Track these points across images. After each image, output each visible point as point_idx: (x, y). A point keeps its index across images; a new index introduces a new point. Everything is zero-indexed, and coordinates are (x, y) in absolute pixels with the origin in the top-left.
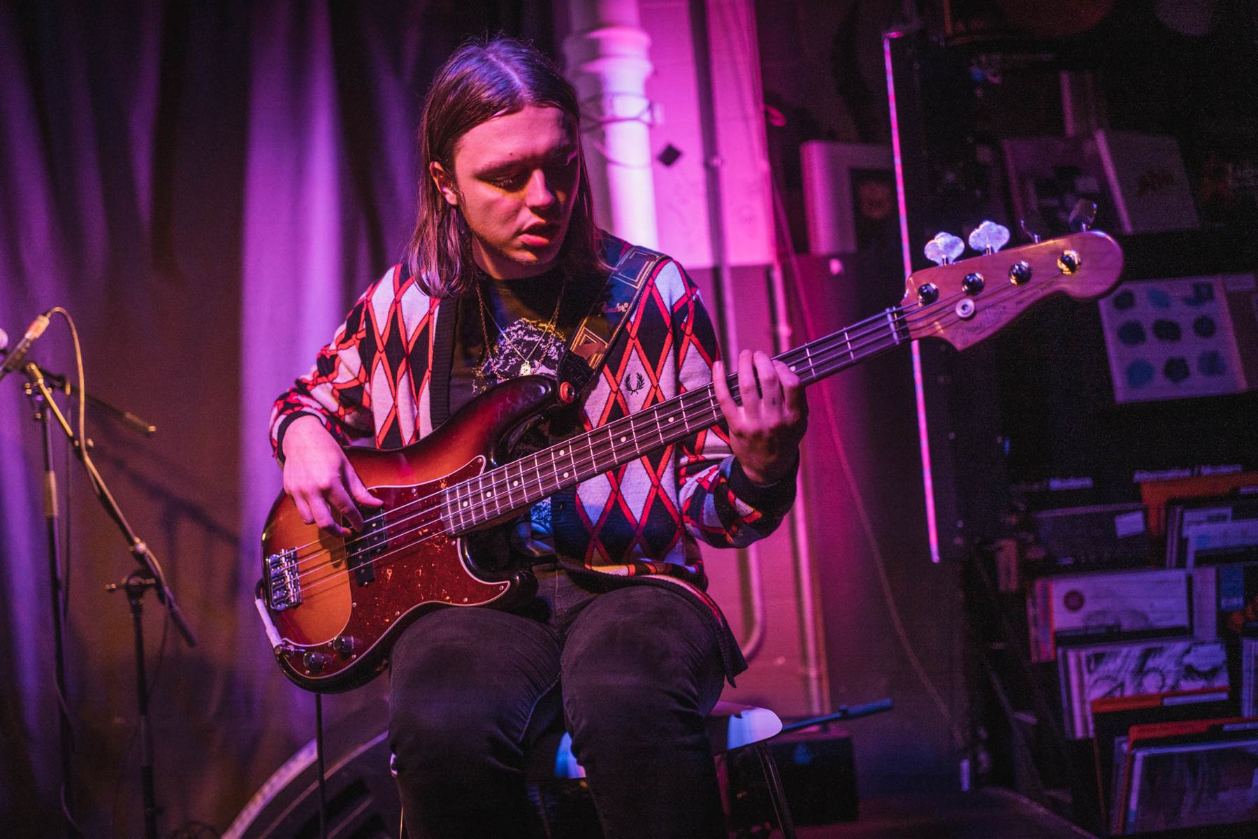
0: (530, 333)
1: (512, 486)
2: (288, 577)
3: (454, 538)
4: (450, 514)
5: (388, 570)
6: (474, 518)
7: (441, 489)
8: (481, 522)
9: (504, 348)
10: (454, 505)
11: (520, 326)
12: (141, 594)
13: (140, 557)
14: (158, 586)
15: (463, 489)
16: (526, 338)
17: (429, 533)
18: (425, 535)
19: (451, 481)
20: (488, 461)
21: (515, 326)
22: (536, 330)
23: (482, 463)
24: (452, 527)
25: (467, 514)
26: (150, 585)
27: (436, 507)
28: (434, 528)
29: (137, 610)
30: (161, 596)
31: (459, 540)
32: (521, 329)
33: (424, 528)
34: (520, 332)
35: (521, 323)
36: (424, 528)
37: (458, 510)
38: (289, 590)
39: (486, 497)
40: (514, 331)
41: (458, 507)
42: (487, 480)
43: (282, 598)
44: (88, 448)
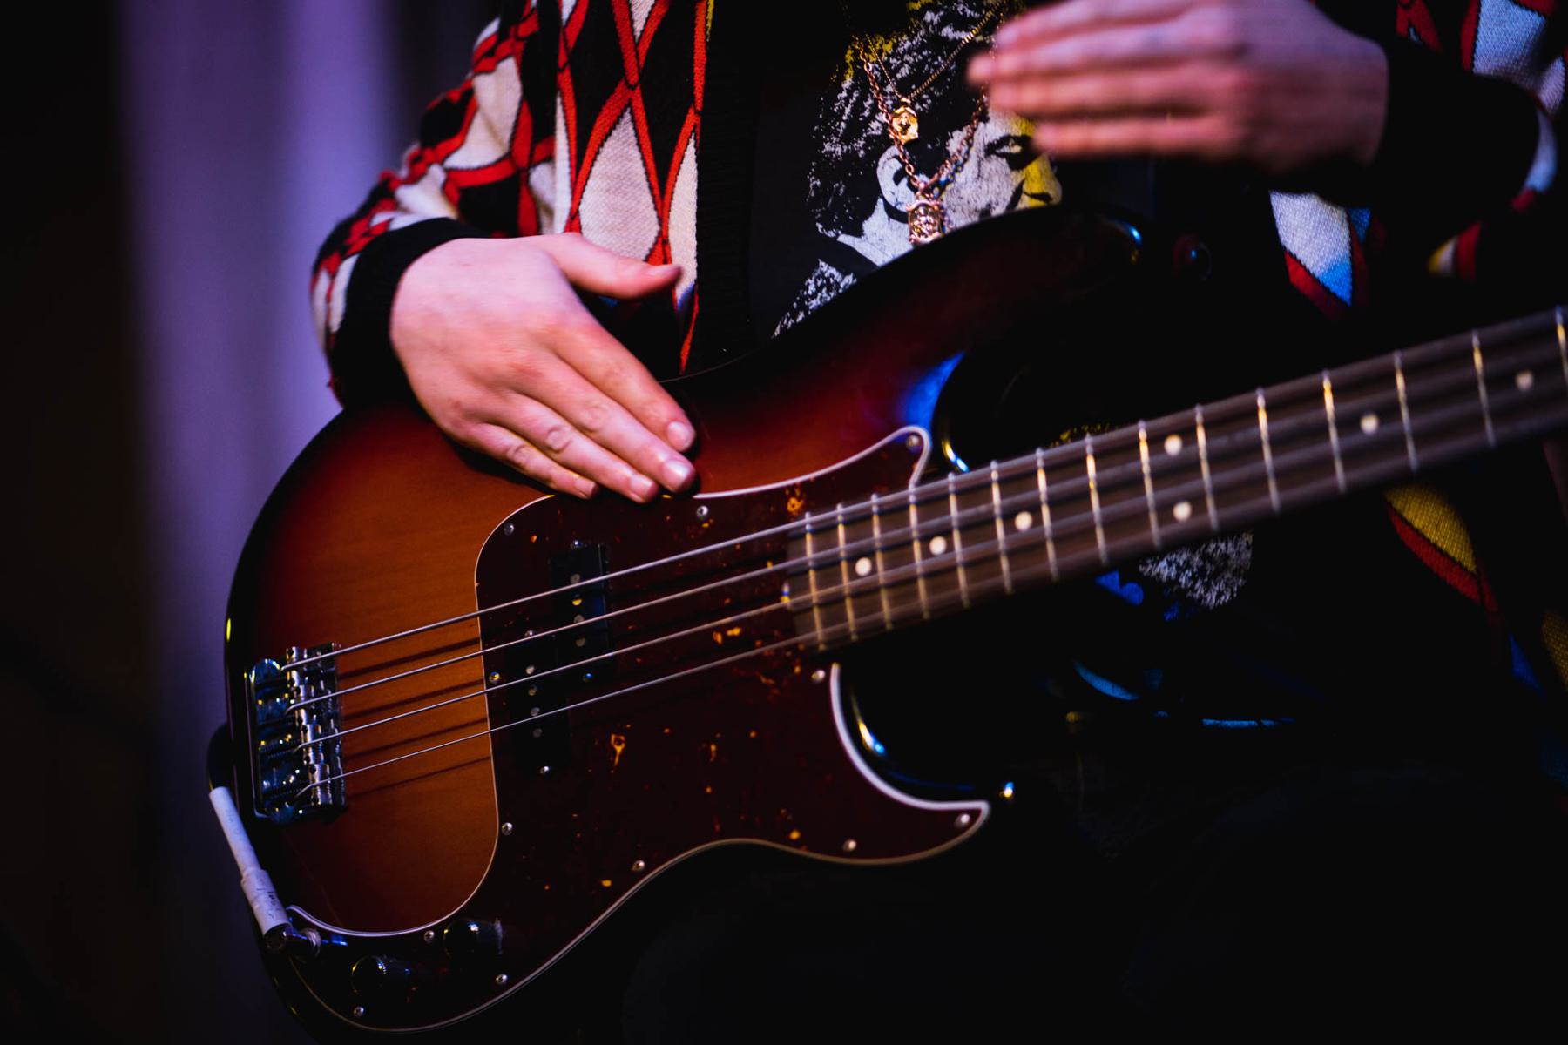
5: (613, 737)
6: (886, 610)
7: (788, 518)
10: (828, 569)
15: (858, 523)
16: (947, 31)
18: (732, 645)
20: (937, 452)
22: (977, 15)
24: (819, 632)
25: (866, 594)
31: (835, 669)
33: (731, 626)
36: (731, 626)
37: (840, 581)
39: (927, 553)
41: (839, 574)
42: (932, 504)
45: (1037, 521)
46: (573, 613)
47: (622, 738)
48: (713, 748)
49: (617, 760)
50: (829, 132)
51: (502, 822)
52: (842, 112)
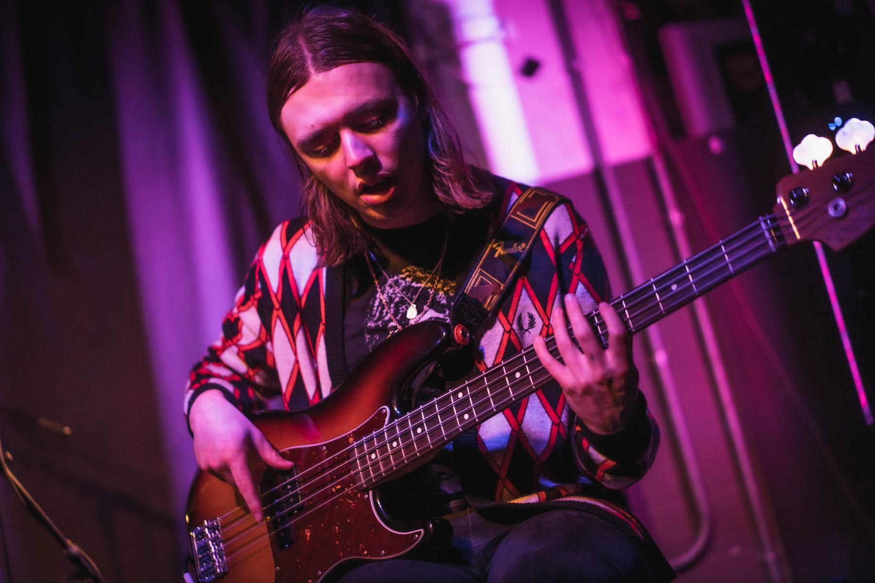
0: (418, 280)
2: (213, 548)
3: (366, 491)
5: (306, 530)
7: (349, 444)
9: (393, 296)
10: (363, 458)
11: (407, 273)
15: (370, 441)
16: (414, 284)
17: (342, 489)
18: (338, 491)
19: (357, 435)
21: (403, 274)
22: (423, 276)
23: (386, 413)
25: (375, 464)
27: (346, 462)
28: (345, 484)
31: (371, 492)
32: (409, 276)
34: (408, 279)
35: (407, 271)
36: (337, 485)
38: (215, 561)
39: (392, 447)
40: (402, 279)
41: (366, 460)
42: (391, 430)
43: (208, 570)
45: (423, 430)
46: (288, 491)
47: (309, 530)
48: (337, 528)
49: (308, 538)
50: (370, 320)
51: (276, 566)
52: (376, 314)
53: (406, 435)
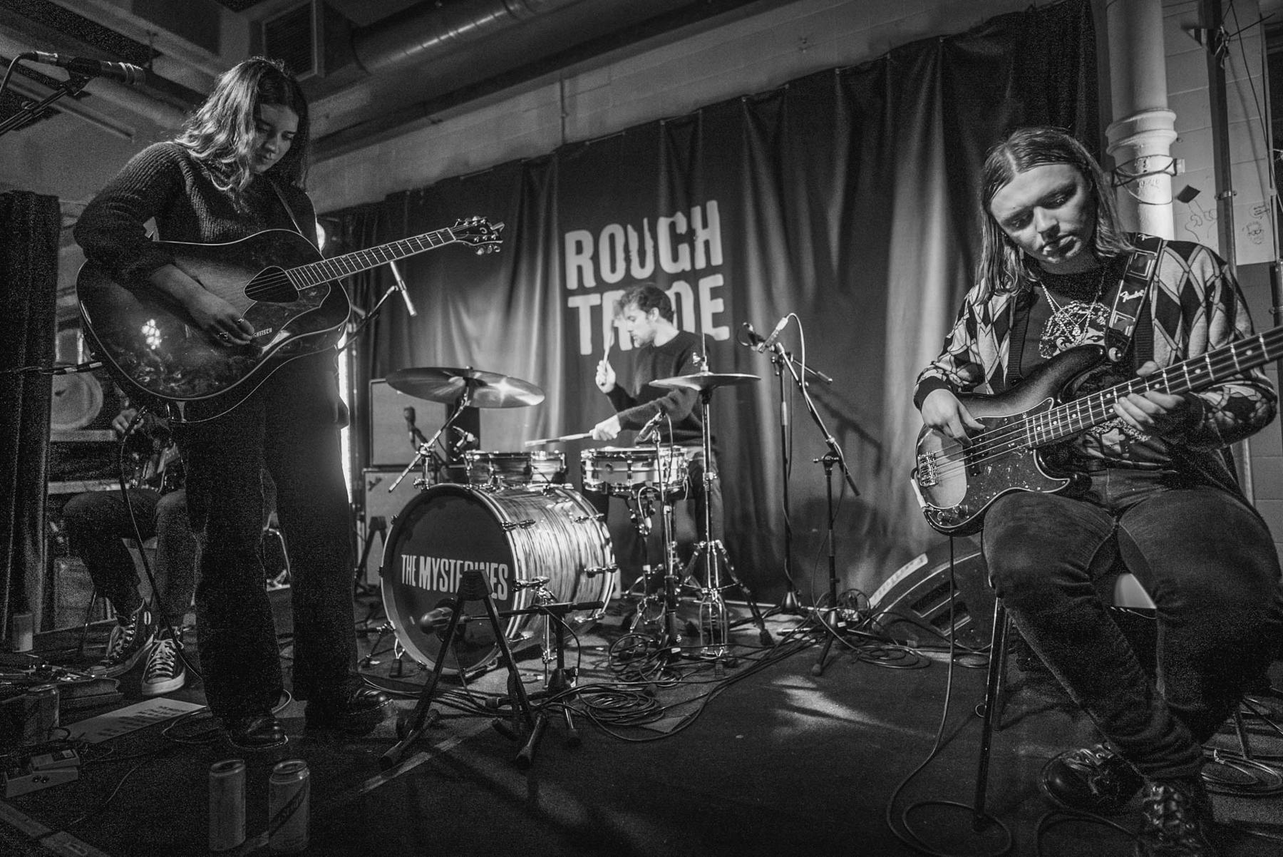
1: (1071, 417)
3: (1032, 449)
4: (1028, 435)
6: (1044, 438)
8: (1050, 440)
10: (1031, 430)
12: (831, 466)
13: (831, 445)
14: (840, 461)
19: (1030, 413)
24: (1030, 443)
25: (1040, 435)
26: (836, 461)
28: (1017, 443)
29: (829, 473)
30: (842, 467)
44: (806, 387)
53: (1064, 418)
